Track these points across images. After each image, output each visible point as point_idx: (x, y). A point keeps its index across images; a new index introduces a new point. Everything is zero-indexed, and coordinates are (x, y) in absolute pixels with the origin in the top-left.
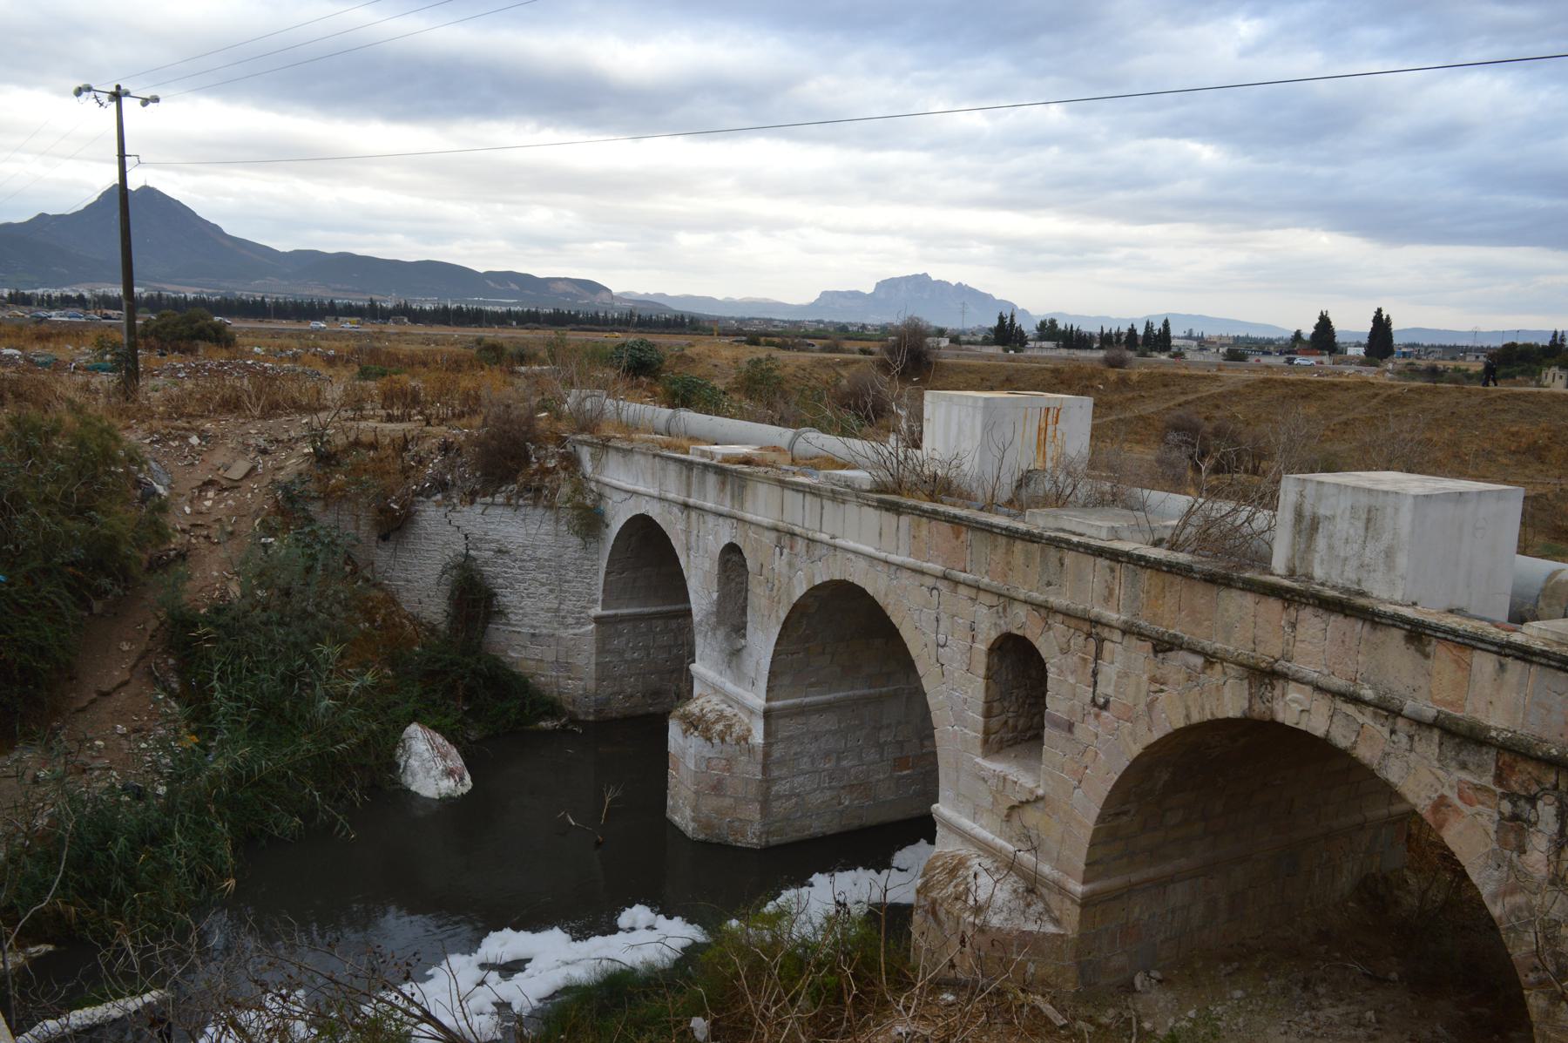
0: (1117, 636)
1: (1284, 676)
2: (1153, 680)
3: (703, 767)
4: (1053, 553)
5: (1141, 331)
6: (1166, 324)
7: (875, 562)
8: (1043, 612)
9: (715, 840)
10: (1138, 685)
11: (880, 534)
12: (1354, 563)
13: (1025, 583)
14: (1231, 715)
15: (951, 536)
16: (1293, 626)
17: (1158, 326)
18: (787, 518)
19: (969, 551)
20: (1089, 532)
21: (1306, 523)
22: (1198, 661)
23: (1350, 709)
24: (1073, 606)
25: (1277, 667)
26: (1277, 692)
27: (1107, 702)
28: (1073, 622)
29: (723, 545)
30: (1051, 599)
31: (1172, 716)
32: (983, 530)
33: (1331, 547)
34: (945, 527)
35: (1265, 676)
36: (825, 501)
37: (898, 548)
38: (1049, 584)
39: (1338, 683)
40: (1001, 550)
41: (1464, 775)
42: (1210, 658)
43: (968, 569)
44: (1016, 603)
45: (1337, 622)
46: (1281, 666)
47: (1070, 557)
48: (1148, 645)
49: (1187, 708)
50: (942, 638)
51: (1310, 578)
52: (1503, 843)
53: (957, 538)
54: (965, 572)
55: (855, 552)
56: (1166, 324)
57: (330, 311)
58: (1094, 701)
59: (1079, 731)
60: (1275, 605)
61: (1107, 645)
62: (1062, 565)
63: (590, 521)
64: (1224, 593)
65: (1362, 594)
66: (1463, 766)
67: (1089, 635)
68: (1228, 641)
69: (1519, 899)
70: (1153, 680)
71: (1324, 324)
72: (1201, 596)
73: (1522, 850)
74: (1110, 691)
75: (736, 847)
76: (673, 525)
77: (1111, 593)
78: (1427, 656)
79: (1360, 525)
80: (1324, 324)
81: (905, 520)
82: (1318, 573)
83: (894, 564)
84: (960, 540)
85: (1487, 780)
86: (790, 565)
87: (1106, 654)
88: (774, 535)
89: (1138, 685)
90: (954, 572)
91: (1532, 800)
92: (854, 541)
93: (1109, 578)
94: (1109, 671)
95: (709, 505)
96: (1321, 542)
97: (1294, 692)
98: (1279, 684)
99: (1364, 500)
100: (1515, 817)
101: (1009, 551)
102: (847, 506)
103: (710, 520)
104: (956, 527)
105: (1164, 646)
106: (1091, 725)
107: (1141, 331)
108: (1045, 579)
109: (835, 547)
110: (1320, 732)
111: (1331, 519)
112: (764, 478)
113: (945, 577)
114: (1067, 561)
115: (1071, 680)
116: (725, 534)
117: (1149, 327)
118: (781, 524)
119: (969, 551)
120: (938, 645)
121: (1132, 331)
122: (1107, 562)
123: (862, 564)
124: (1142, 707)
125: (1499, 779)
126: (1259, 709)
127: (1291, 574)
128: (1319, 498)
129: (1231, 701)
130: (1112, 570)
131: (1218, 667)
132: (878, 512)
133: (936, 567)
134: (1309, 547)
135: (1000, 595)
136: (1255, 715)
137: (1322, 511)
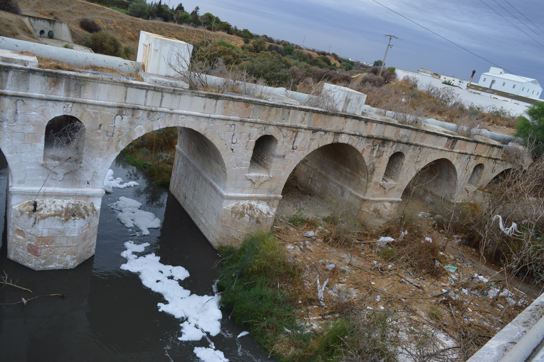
1: (343, 133)
2: (311, 139)
3: (81, 232)
4: (287, 111)
7: (200, 118)
8: (280, 127)
9: (82, 262)
10: (307, 142)
11: (204, 107)
12: (355, 108)
13: (275, 119)
14: (329, 143)
15: (244, 106)
16: (346, 122)
18: (148, 104)
19: (252, 111)
20: (293, 103)
21: (348, 100)
22: (323, 133)
23: (353, 137)
24: (292, 125)
26: (340, 137)
27: (297, 147)
28: (290, 129)
29: (53, 117)
30: (285, 123)
31: (315, 146)
32: (259, 104)
33: (351, 105)
34: (242, 104)
35: (338, 134)
36: (164, 94)
37: (215, 112)
38: (284, 119)
39: (352, 133)
40: (266, 111)
41: (368, 144)
42: (326, 132)
43: (250, 117)
44: (270, 126)
45: (354, 121)
46: (342, 131)
47: (292, 111)
48: (311, 131)
49: (319, 144)
50: (234, 141)
51: (346, 112)
52: (370, 153)
53: (247, 107)
54: (249, 118)
55: (186, 115)
57: (227, 28)
58: (293, 149)
59: (286, 157)
60: (343, 118)
61: (299, 133)
62: (289, 114)
64: (333, 117)
66: (368, 143)
67: (294, 132)
68: (331, 128)
69: (371, 161)
70: (311, 139)
72: (327, 118)
73: (373, 154)
74: (298, 144)
75: (90, 258)
77: (304, 119)
78: (367, 125)
79: (357, 101)
81: (220, 102)
82: (348, 111)
83: (212, 118)
84: (248, 108)
85: (371, 144)
86: (131, 123)
87: (299, 136)
88: (118, 109)
89: (307, 142)
90: (245, 119)
91: (376, 146)
92: (186, 110)
93: (304, 116)
94: (299, 140)
96: (349, 104)
97: (343, 136)
98: (340, 135)
99: (359, 96)
100: (373, 149)
101: (270, 111)
102: (182, 96)
103: (34, 104)
104: (247, 104)
105: (315, 131)
106: (291, 154)
108: (282, 118)
109: (172, 114)
110: (346, 142)
111: (352, 100)
112: (109, 81)
113: (241, 121)
114: (291, 113)
115: (286, 144)
118: (125, 104)
119: (252, 111)
120: (232, 143)
122: (304, 112)
123: (191, 119)
124: (307, 146)
125: (373, 143)
126: (336, 141)
127: (343, 111)
128: (351, 95)
129: (329, 140)
130: (305, 114)
131: (328, 134)
132: (204, 99)
133: (237, 118)
134: (347, 106)
135: (264, 124)
136: (334, 142)
137: (351, 98)
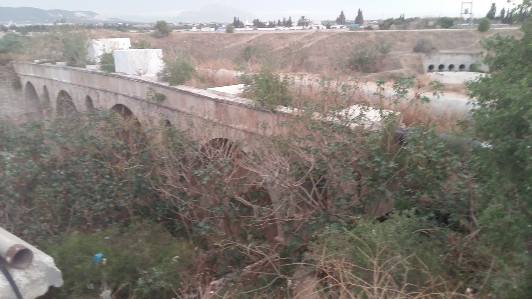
0: (99, 91)
5: (282, 20)
6: (290, 18)
17: (287, 19)
25: (117, 92)
45: (122, 80)
56: (290, 18)
63: (17, 85)
65: (125, 74)
71: (342, 15)
76: (34, 82)
80: (342, 15)
95: (38, 75)
105: (105, 91)
107: (282, 20)
116: (42, 83)
117: (284, 19)
121: (279, 21)
